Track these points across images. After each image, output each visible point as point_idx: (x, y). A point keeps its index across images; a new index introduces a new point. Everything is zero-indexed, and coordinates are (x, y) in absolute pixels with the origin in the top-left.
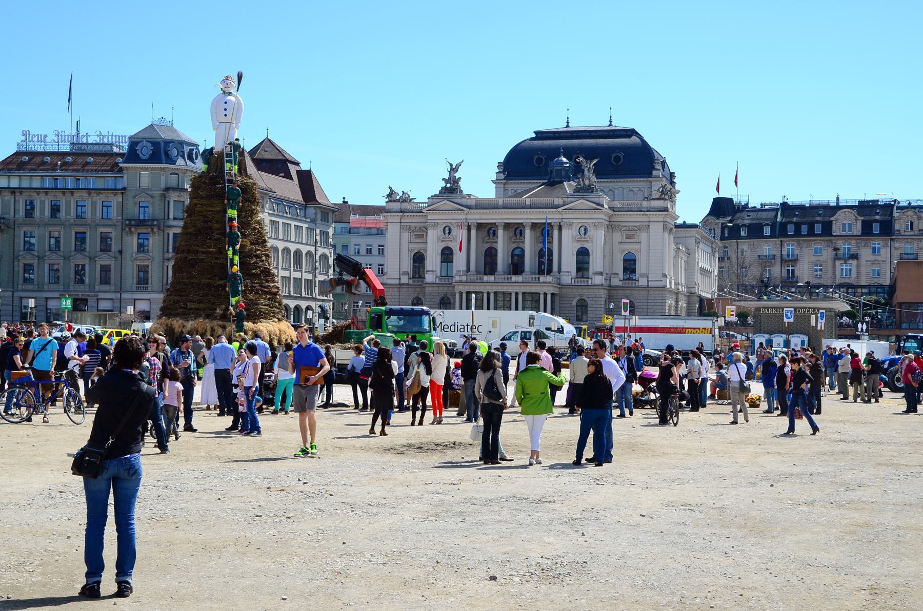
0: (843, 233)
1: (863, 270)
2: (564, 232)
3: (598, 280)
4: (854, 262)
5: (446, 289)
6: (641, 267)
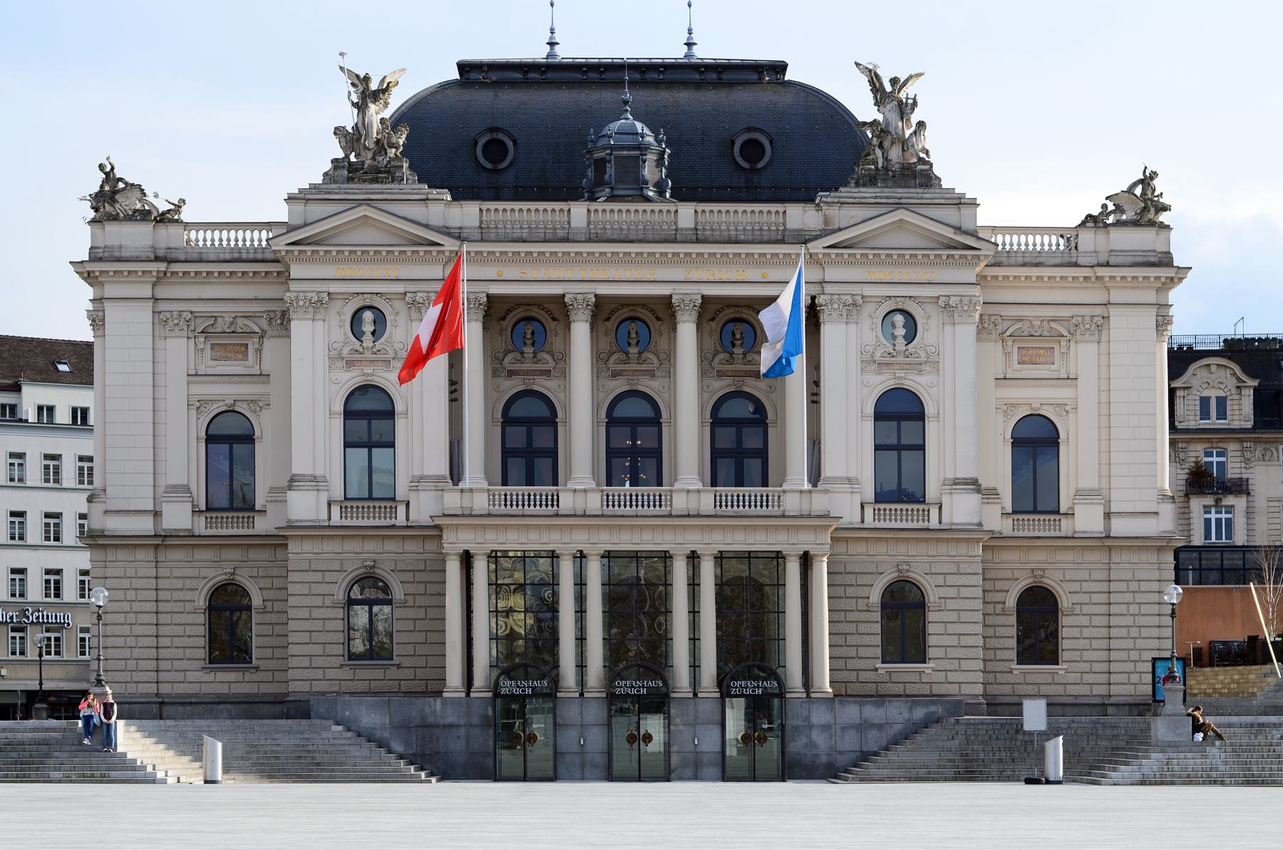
0: (1204, 424)
1: (1261, 523)
2: (831, 332)
3: (962, 510)
4: (1239, 503)
5: (370, 546)
6: (1076, 466)
